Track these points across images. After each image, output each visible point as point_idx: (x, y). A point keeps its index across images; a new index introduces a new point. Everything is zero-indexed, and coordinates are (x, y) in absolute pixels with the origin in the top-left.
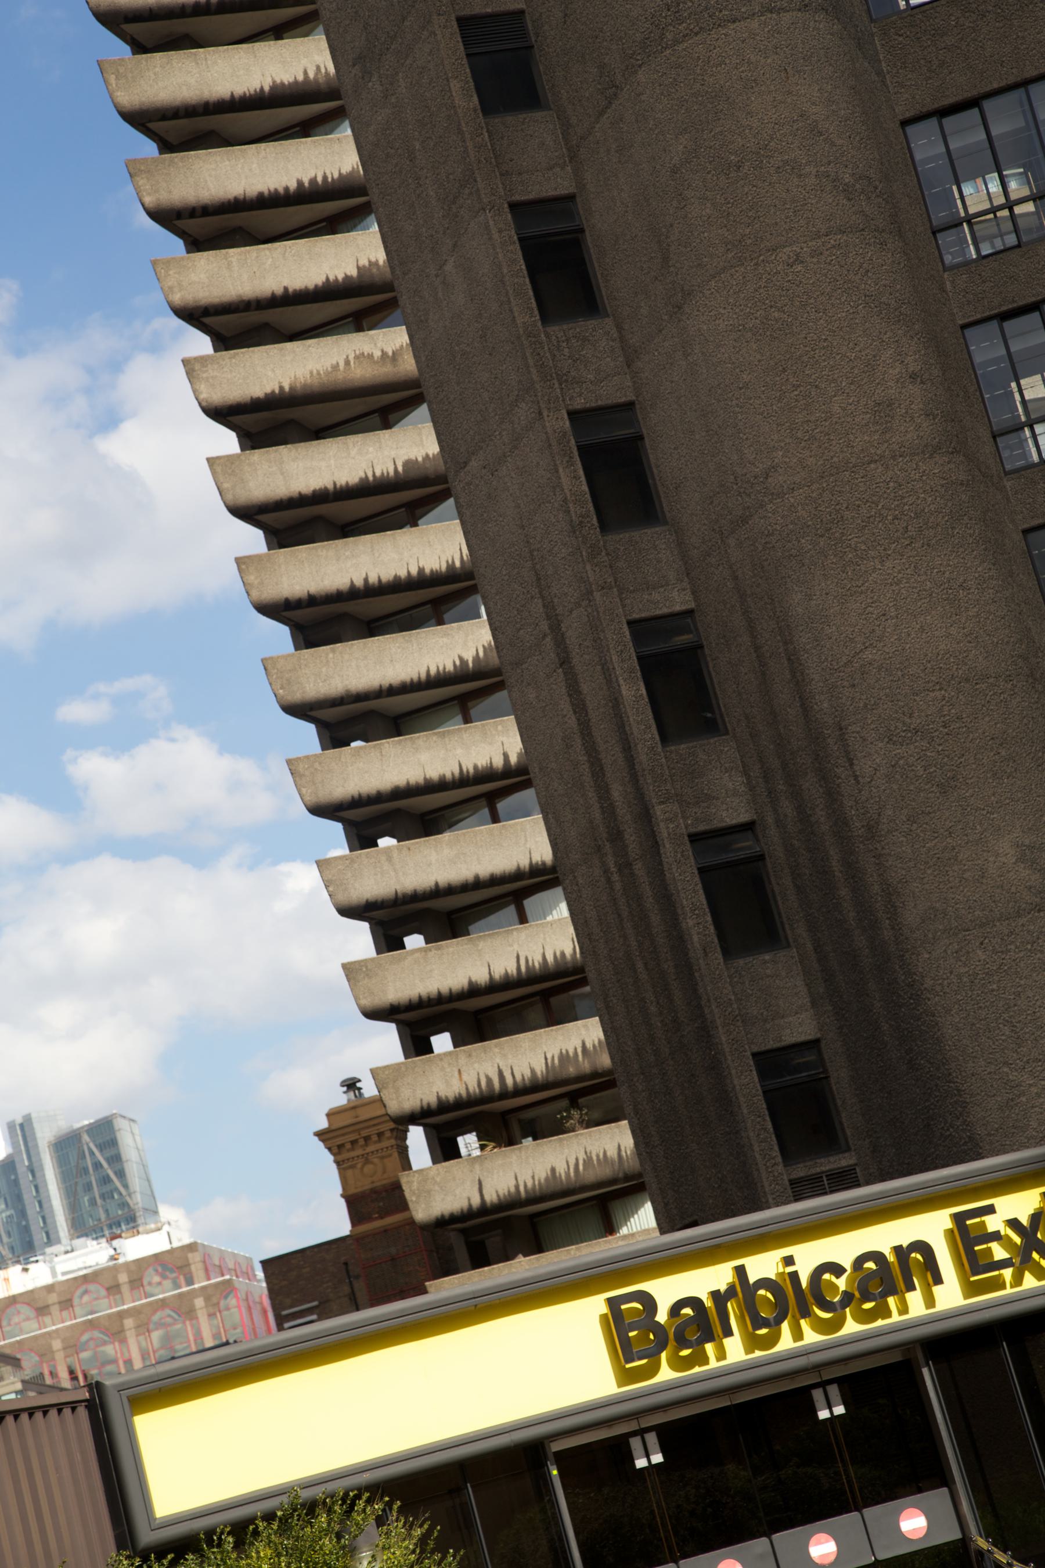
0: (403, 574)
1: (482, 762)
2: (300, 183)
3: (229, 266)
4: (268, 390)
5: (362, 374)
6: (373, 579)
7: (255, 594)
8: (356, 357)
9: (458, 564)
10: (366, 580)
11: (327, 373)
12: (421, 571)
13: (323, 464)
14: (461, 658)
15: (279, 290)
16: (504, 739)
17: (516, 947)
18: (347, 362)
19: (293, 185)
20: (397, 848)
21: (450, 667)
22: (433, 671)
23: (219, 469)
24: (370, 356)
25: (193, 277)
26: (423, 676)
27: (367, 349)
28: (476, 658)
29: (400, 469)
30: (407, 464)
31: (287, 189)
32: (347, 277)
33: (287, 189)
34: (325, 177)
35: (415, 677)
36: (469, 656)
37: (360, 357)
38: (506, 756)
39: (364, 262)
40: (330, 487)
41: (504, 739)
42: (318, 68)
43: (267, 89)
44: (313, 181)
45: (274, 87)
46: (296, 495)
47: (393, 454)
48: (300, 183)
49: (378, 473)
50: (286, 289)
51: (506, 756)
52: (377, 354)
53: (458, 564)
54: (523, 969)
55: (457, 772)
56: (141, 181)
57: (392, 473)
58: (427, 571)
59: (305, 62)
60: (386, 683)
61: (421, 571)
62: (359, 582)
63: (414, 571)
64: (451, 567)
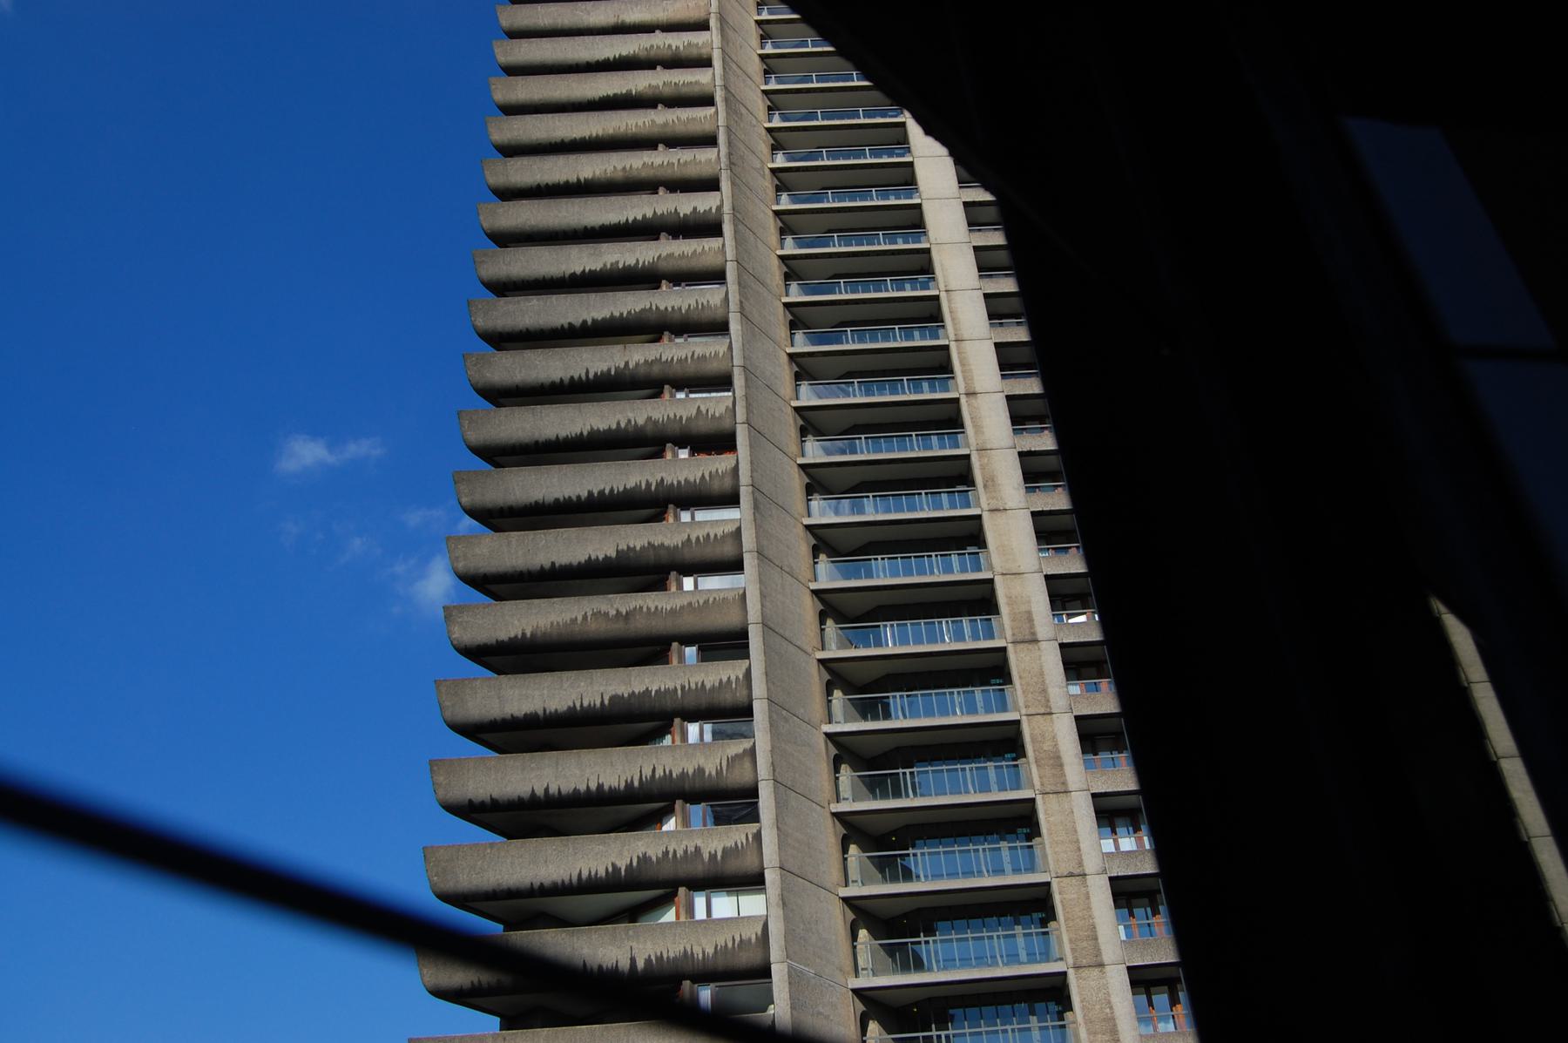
0: (582, 788)
2: (590, 493)
3: (509, 543)
5: (597, 628)
6: (553, 790)
7: (441, 793)
9: (636, 784)
10: (547, 790)
12: (600, 787)
13: (537, 693)
15: (547, 565)
16: (634, 944)
18: (585, 617)
19: (584, 494)
20: (495, 1036)
21: (602, 873)
22: (585, 874)
23: (443, 690)
24: (606, 614)
25: (477, 551)
26: (575, 879)
27: (604, 608)
28: (629, 867)
30: (611, 699)
33: (579, 497)
34: (612, 490)
35: (567, 880)
36: (622, 864)
38: (633, 960)
39: (623, 547)
40: (541, 712)
41: (634, 944)
44: (601, 493)
45: (592, 433)
47: (602, 689)
48: (590, 493)
49: (586, 704)
51: (633, 960)
53: (636, 784)
56: (463, 487)
57: (598, 703)
58: (606, 787)
59: (619, 417)
60: (537, 885)
61: (600, 787)
62: (540, 792)
63: (593, 786)
64: (629, 785)
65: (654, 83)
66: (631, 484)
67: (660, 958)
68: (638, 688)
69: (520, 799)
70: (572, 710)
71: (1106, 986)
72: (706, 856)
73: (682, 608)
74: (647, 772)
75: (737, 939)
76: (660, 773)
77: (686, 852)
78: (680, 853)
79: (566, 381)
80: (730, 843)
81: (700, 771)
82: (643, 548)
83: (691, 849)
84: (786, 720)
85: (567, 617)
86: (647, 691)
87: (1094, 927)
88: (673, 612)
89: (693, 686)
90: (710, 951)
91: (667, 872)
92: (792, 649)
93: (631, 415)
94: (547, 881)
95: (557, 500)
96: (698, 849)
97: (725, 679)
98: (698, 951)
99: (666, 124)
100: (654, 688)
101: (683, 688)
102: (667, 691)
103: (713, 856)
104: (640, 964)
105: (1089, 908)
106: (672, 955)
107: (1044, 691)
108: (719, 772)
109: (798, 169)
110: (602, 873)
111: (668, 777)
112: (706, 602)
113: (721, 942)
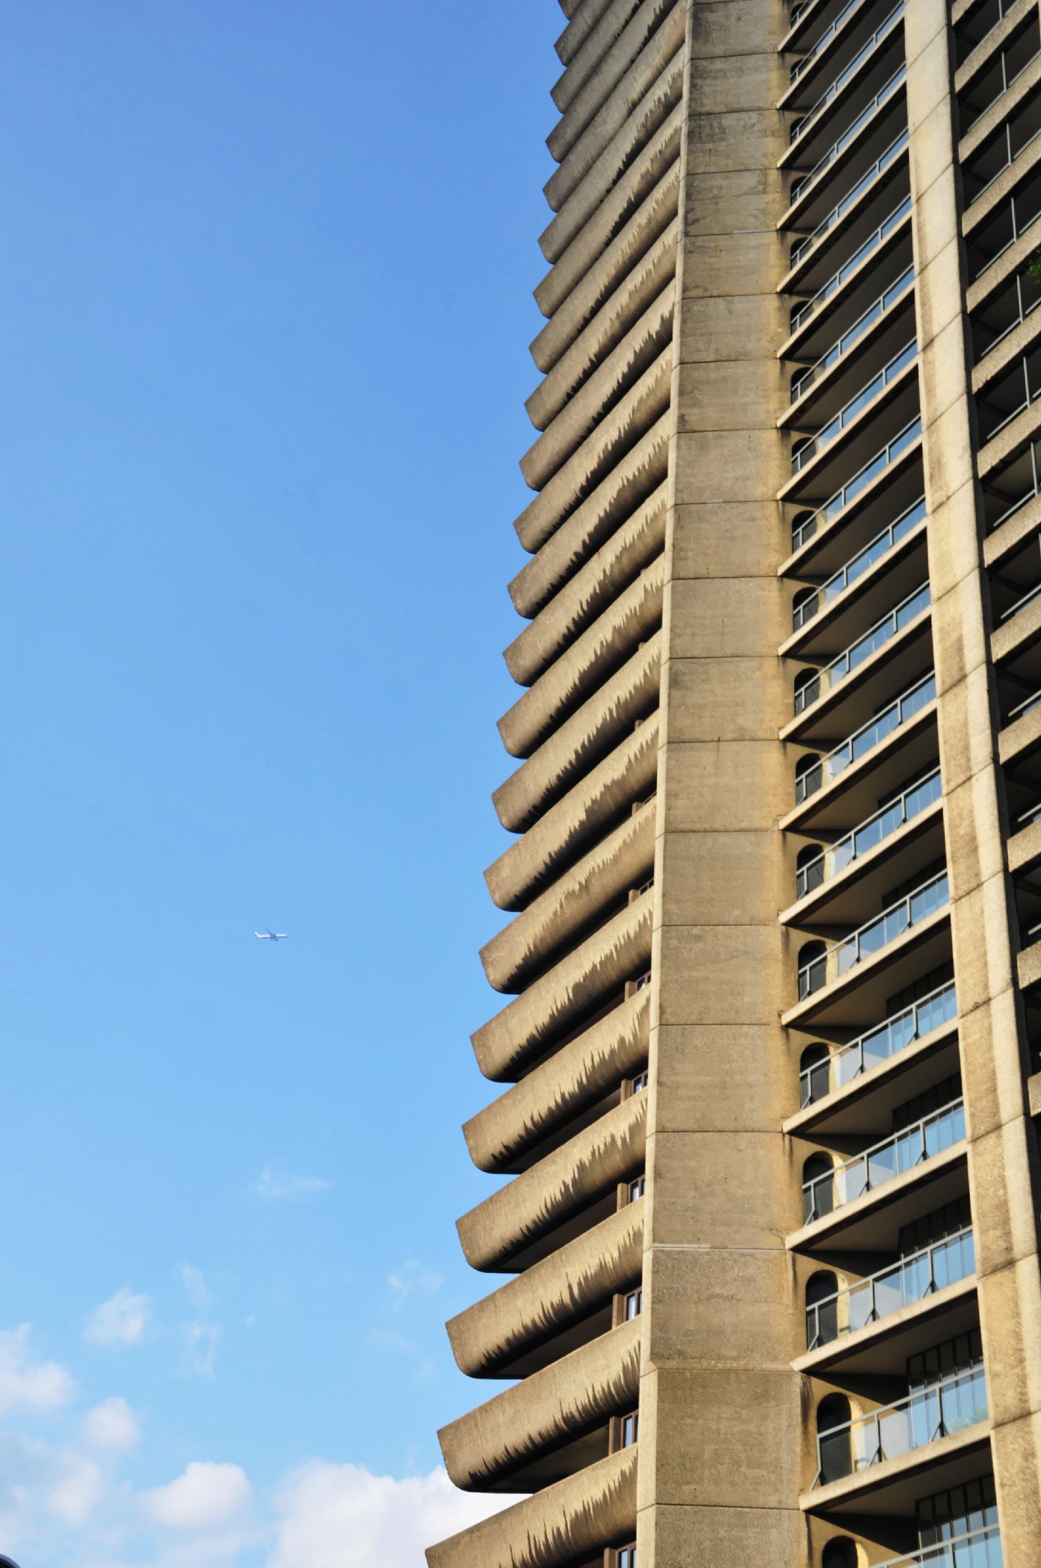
1: (556, 1300)
2: (576, 752)
4: (523, 955)
5: (576, 911)
6: (536, 1118)
8: (566, 898)
9: (585, 1081)
11: (552, 921)
14: (564, 1183)
17: (526, 1525)
19: (573, 757)
24: (573, 891)
25: (504, 875)
26: (544, 1211)
29: (571, 996)
31: (570, 763)
32: (582, 823)
37: (570, 895)
42: (602, 643)
43: (577, 682)
44: (583, 746)
46: (519, 1049)
50: (550, 854)
52: (577, 887)
54: (533, 1551)
55: (541, 1315)
58: (567, 1095)
62: (529, 1124)
63: (559, 1100)
64: (580, 1084)
65: (643, 170)
66: (599, 722)
67: (586, 1278)
68: (587, 968)
69: (521, 1137)
70: (552, 1016)
71: (1001, 1156)
72: (619, 1142)
73: (620, 850)
74: (589, 1064)
75: (631, 1233)
76: (597, 1060)
77: (605, 1144)
78: (602, 1147)
79: (572, 627)
80: (632, 1120)
81: (622, 1040)
82: (602, 794)
83: (609, 1139)
84: (698, 938)
85: (550, 913)
86: (594, 966)
87: (994, 1073)
88: (616, 859)
89: (622, 941)
90: (616, 1255)
91: (598, 1176)
92: (724, 839)
93: (601, 637)
94: (529, 1223)
95: (558, 777)
96: (613, 1138)
97: (641, 919)
98: (608, 1259)
99: (649, 221)
100: (597, 961)
101: (616, 947)
102: (607, 957)
103: (624, 1140)
104: (576, 1292)
105: (991, 1047)
106: (593, 1271)
107: (967, 748)
108: (635, 1036)
109: (806, 141)
110: (559, 1197)
111: (603, 1061)
112: (635, 832)
113: (621, 1243)
